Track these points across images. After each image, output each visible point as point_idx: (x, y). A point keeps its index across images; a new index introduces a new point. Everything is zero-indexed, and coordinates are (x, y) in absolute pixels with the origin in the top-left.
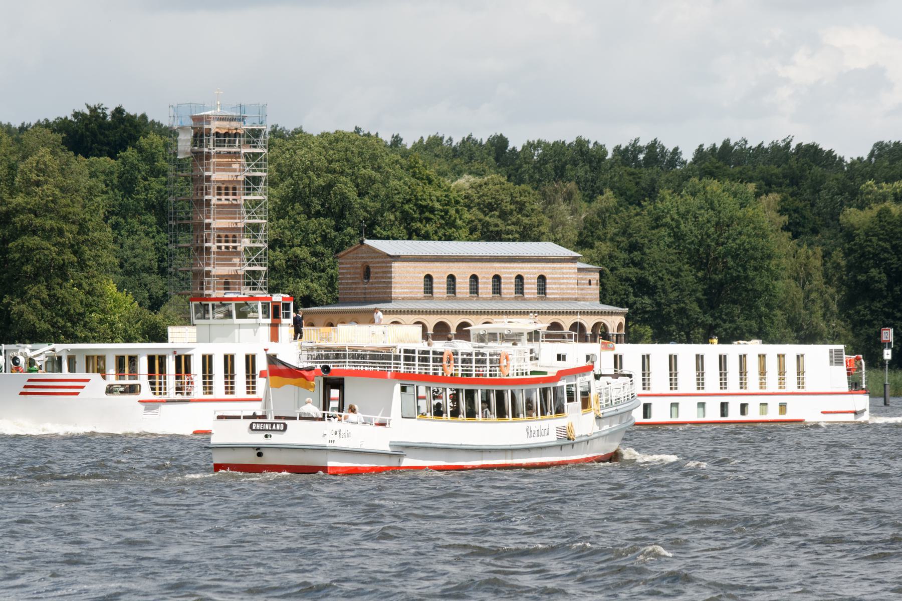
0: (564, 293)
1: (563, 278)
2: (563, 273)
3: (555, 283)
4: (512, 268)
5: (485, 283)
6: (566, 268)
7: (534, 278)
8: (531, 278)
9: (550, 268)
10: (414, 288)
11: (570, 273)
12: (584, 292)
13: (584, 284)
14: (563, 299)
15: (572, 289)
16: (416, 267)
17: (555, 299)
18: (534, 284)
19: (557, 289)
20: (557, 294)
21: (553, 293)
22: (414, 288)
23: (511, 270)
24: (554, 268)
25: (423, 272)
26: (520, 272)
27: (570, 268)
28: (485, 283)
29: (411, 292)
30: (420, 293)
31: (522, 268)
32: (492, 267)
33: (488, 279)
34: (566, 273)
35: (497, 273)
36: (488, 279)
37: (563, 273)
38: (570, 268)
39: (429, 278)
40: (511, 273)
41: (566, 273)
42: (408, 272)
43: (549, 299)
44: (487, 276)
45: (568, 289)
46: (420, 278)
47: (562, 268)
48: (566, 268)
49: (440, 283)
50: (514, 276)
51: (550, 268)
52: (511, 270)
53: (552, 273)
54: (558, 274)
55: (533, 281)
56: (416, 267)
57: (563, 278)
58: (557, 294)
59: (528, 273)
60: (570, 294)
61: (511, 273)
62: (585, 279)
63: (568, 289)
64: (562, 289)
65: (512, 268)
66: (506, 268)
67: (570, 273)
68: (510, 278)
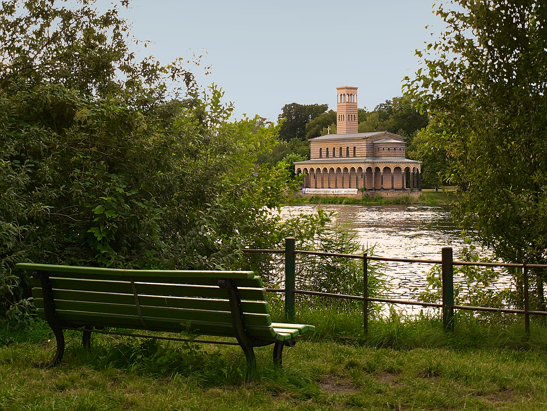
1: (361, 148)
2: (361, 146)
3: (359, 150)
4: (346, 144)
9: (357, 144)
11: (364, 145)
15: (364, 152)
24: (358, 143)
27: (364, 143)
34: (362, 146)
38: (364, 143)
40: (345, 146)
41: (362, 146)
45: (363, 152)
47: (361, 143)
50: (346, 147)
51: (357, 144)
53: (358, 146)
57: (361, 148)
61: (345, 146)
63: (363, 152)
64: (361, 152)
65: (346, 144)
67: (364, 145)
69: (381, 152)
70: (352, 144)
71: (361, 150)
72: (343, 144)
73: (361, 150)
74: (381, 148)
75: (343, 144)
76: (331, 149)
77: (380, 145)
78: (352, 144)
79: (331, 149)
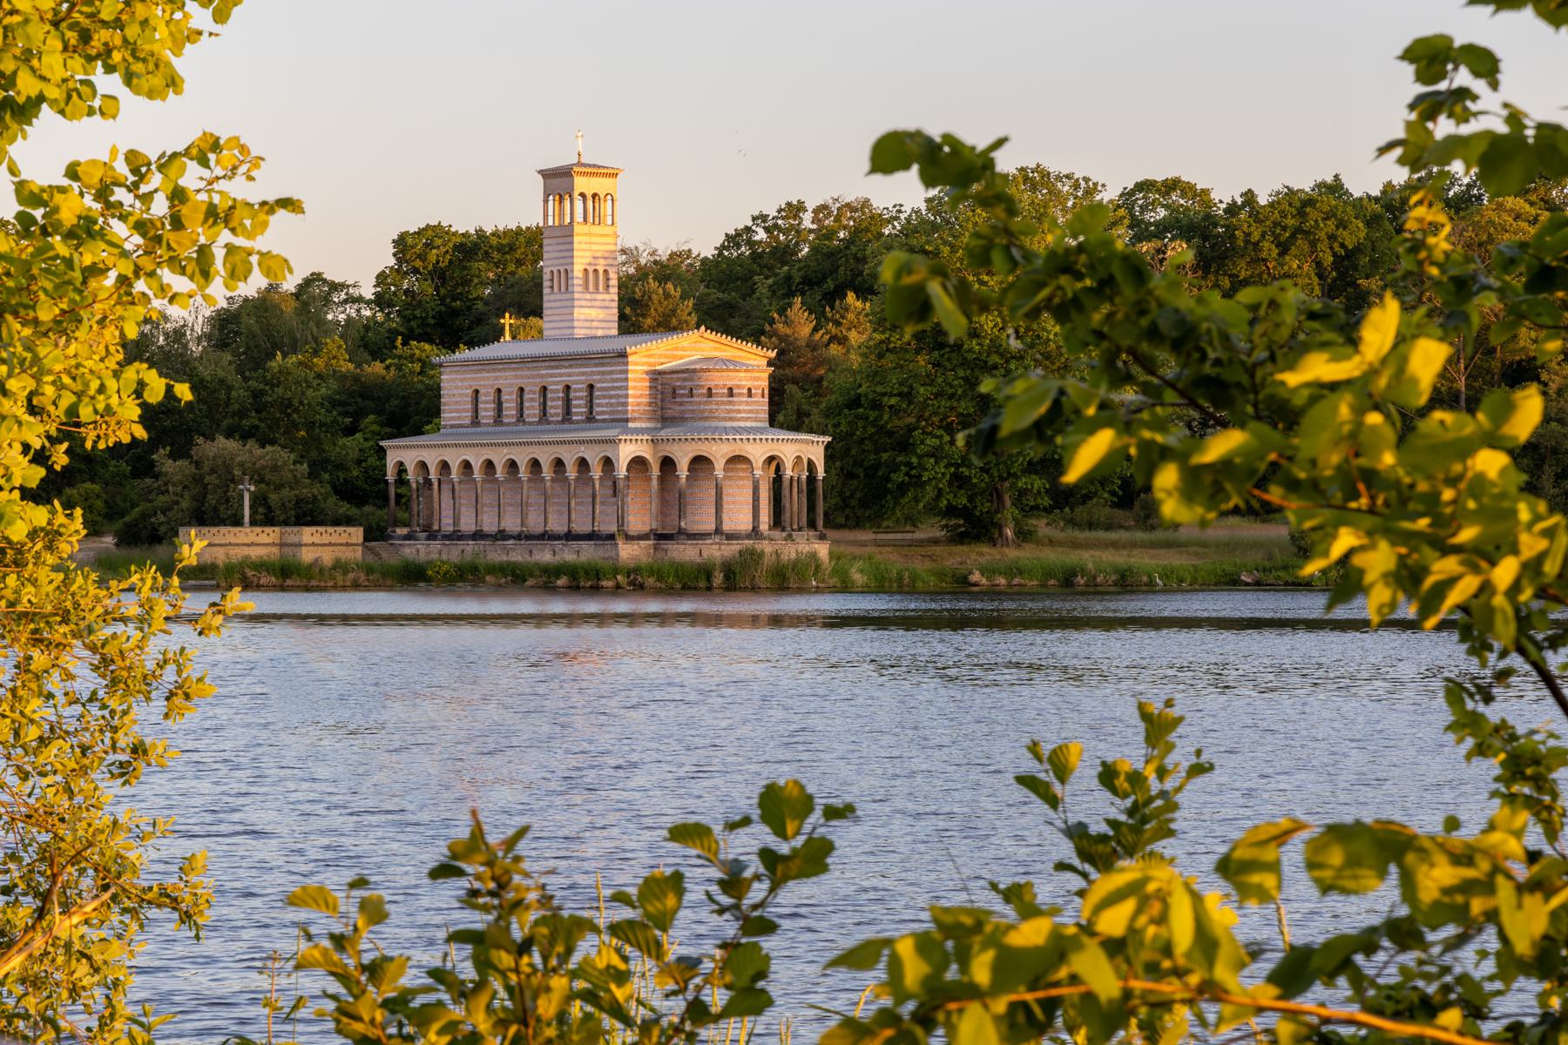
1: (614, 388)
3: (604, 397)
4: (561, 375)
5: (532, 400)
9: (599, 373)
12: (682, 408)
13: (682, 396)
14: (613, 420)
17: (604, 421)
24: (603, 373)
28: (532, 400)
33: (534, 393)
40: (557, 383)
43: (597, 421)
47: (612, 372)
50: (560, 387)
51: (599, 373)
57: (614, 388)
61: (557, 383)
62: (685, 387)
64: (611, 405)
65: (561, 375)
69: (681, 404)
71: (611, 397)
72: (551, 376)
73: (611, 397)
74: (681, 388)
75: (551, 376)
77: (678, 379)
78: (584, 374)
79: (510, 394)
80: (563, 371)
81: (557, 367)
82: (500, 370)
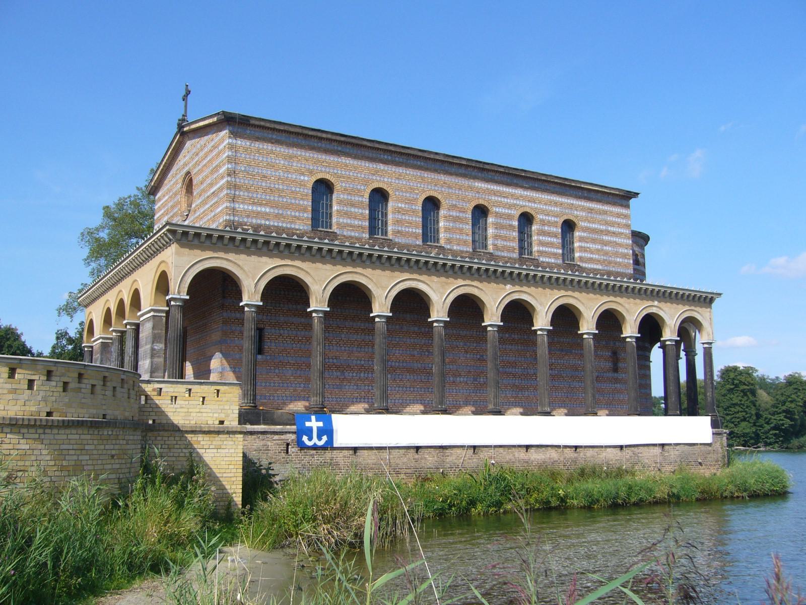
0: (610, 263)
1: (608, 233)
2: (607, 223)
3: (594, 241)
4: (513, 196)
5: (456, 219)
6: (612, 214)
7: (554, 224)
8: (549, 224)
9: (583, 209)
10: (287, 207)
11: (619, 224)
16: (291, 157)
18: (556, 236)
19: (598, 251)
20: (598, 261)
21: (591, 260)
22: (287, 207)
23: (510, 201)
24: (591, 210)
25: (311, 173)
26: (529, 207)
29: (277, 216)
30: (302, 223)
31: (533, 200)
32: (471, 188)
33: (463, 211)
34: (612, 224)
35: (481, 202)
36: (463, 211)
37: (607, 223)
39: (323, 188)
40: (510, 206)
41: (612, 224)
42: (271, 166)
44: (460, 204)
45: (616, 254)
46: (302, 184)
47: (605, 213)
48: (612, 214)
49: (353, 205)
50: (517, 213)
51: (583, 209)
52: (510, 201)
54: (599, 222)
55: (554, 229)
56: (291, 157)
57: (608, 233)
58: (598, 261)
59: (543, 212)
60: (620, 264)
61: (510, 206)
64: (606, 253)
65: (513, 196)
66: (501, 194)
68: (509, 217)
70: (556, 204)
72: (495, 193)
75: (495, 193)
76: (411, 202)
78: (556, 204)
79: (411, 202)
80: (519, 192)
81: (508, 184)
82: (385, 162)
